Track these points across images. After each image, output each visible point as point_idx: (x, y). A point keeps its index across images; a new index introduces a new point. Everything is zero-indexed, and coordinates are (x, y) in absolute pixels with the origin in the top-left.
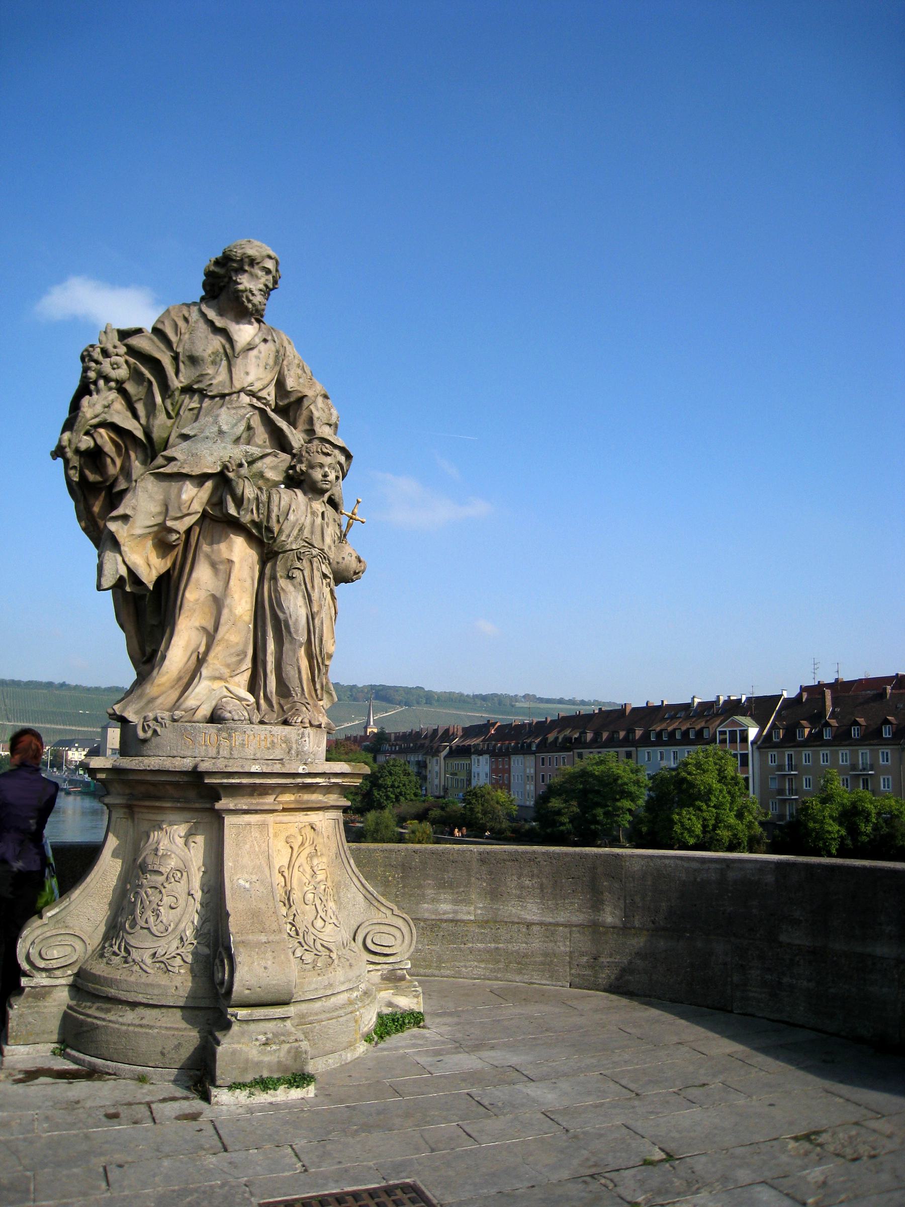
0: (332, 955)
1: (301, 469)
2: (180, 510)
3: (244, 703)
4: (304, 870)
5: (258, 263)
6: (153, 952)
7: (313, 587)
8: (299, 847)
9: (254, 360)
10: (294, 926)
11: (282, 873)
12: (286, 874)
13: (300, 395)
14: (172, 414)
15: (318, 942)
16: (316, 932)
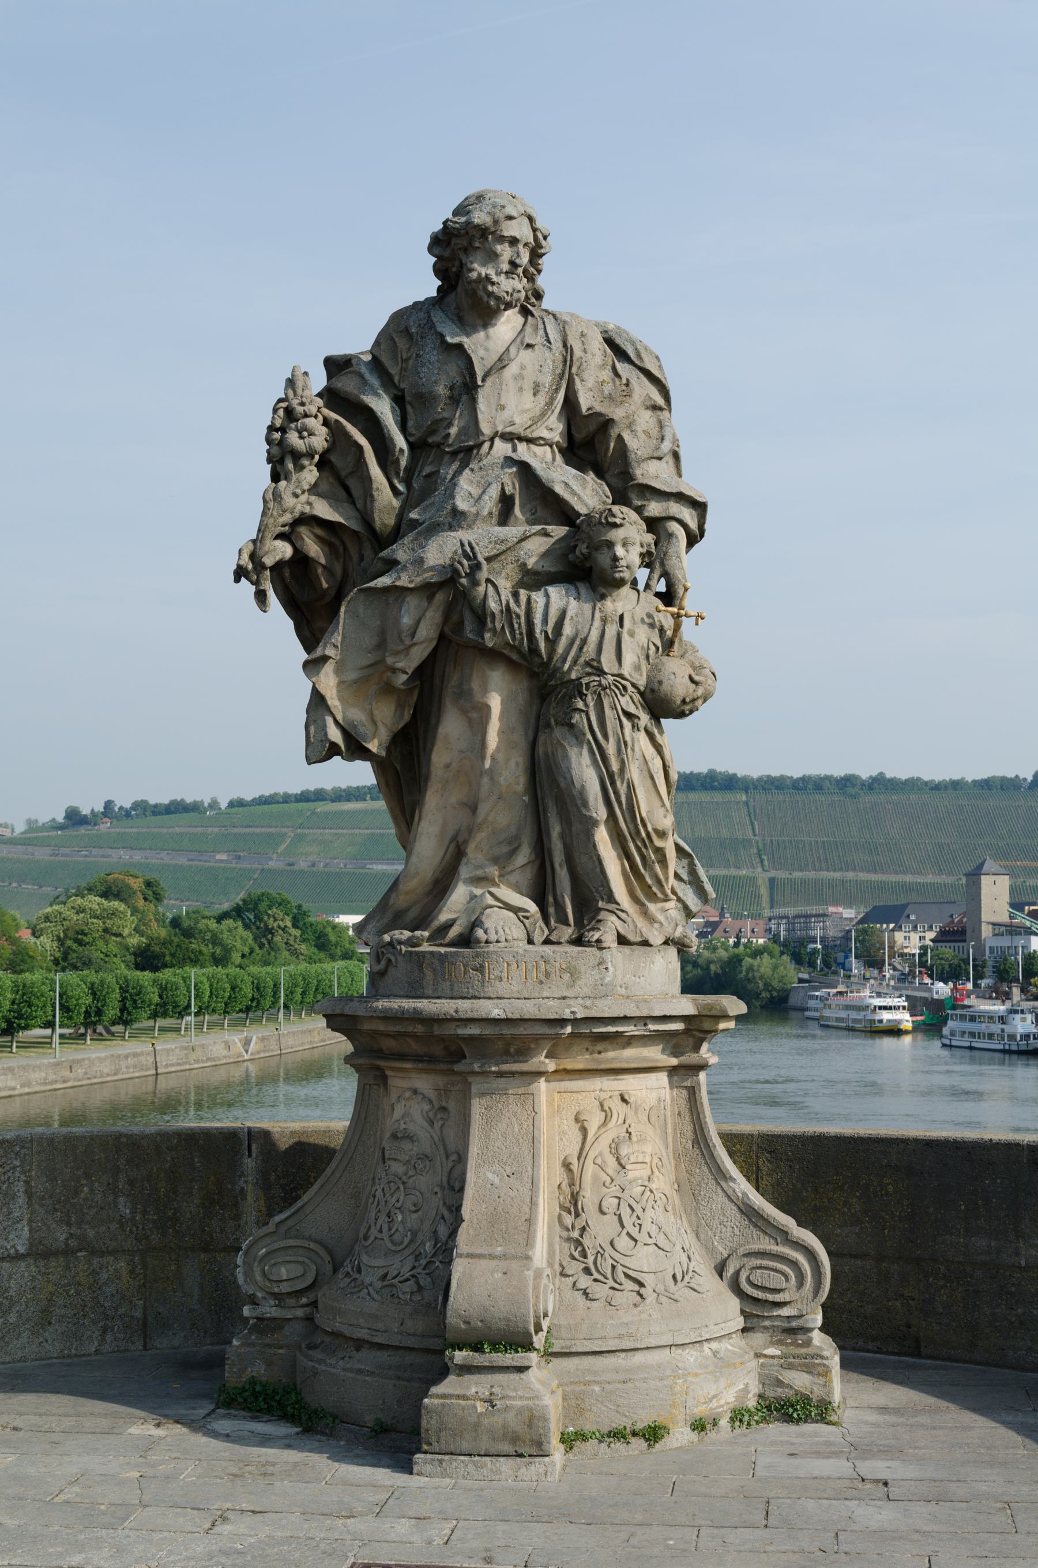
0: (643, 1291)
1: (583, 554)
2: (402, 641)
3: (520, 914)
4: (604, 1161)
5: (493, 233)
6: (385, 1271)
7: (606, 736)
8: (599, 1128)
9: (511, 383)
10: (581, 1244)
11: (567, 1165)
12: (575, 1167)
13: (601, 419)
14: (401, 487)
15: (620, 1269)
16: (617, 1256)
